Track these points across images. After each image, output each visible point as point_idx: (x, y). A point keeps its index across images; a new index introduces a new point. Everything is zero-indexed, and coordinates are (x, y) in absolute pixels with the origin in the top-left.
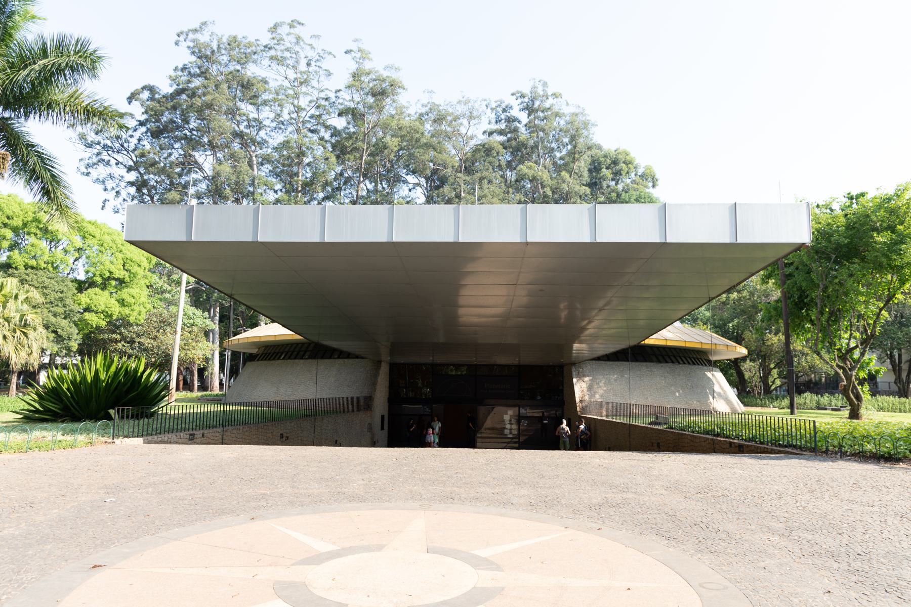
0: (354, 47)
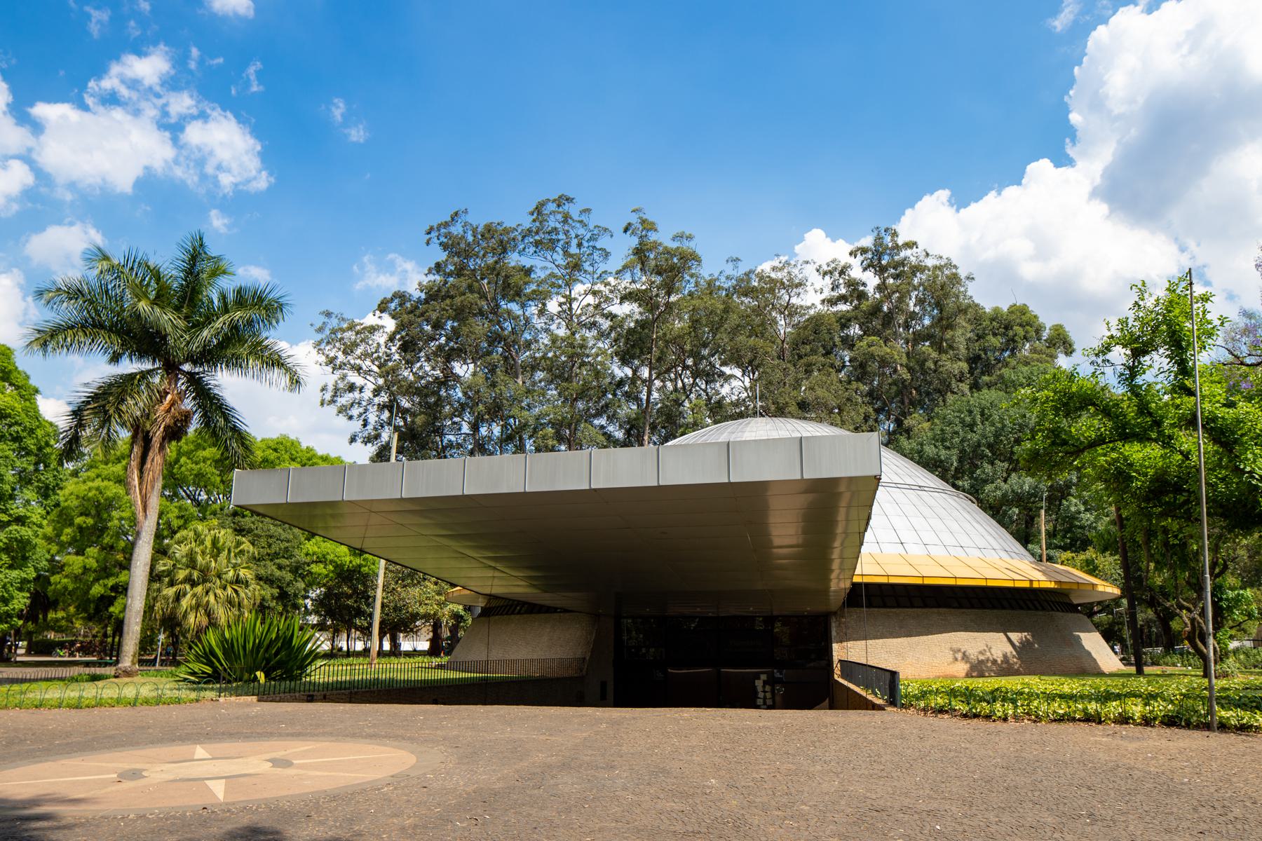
0: (634, 219)
